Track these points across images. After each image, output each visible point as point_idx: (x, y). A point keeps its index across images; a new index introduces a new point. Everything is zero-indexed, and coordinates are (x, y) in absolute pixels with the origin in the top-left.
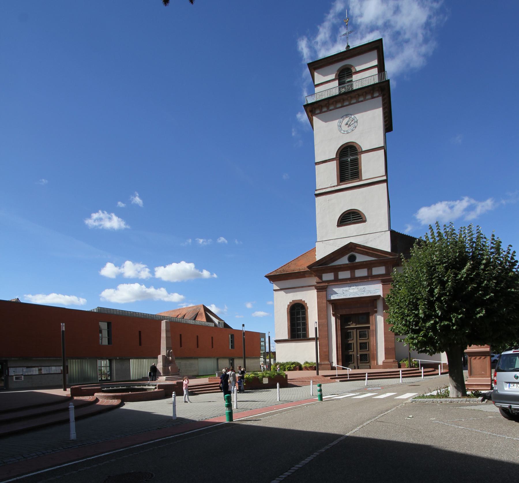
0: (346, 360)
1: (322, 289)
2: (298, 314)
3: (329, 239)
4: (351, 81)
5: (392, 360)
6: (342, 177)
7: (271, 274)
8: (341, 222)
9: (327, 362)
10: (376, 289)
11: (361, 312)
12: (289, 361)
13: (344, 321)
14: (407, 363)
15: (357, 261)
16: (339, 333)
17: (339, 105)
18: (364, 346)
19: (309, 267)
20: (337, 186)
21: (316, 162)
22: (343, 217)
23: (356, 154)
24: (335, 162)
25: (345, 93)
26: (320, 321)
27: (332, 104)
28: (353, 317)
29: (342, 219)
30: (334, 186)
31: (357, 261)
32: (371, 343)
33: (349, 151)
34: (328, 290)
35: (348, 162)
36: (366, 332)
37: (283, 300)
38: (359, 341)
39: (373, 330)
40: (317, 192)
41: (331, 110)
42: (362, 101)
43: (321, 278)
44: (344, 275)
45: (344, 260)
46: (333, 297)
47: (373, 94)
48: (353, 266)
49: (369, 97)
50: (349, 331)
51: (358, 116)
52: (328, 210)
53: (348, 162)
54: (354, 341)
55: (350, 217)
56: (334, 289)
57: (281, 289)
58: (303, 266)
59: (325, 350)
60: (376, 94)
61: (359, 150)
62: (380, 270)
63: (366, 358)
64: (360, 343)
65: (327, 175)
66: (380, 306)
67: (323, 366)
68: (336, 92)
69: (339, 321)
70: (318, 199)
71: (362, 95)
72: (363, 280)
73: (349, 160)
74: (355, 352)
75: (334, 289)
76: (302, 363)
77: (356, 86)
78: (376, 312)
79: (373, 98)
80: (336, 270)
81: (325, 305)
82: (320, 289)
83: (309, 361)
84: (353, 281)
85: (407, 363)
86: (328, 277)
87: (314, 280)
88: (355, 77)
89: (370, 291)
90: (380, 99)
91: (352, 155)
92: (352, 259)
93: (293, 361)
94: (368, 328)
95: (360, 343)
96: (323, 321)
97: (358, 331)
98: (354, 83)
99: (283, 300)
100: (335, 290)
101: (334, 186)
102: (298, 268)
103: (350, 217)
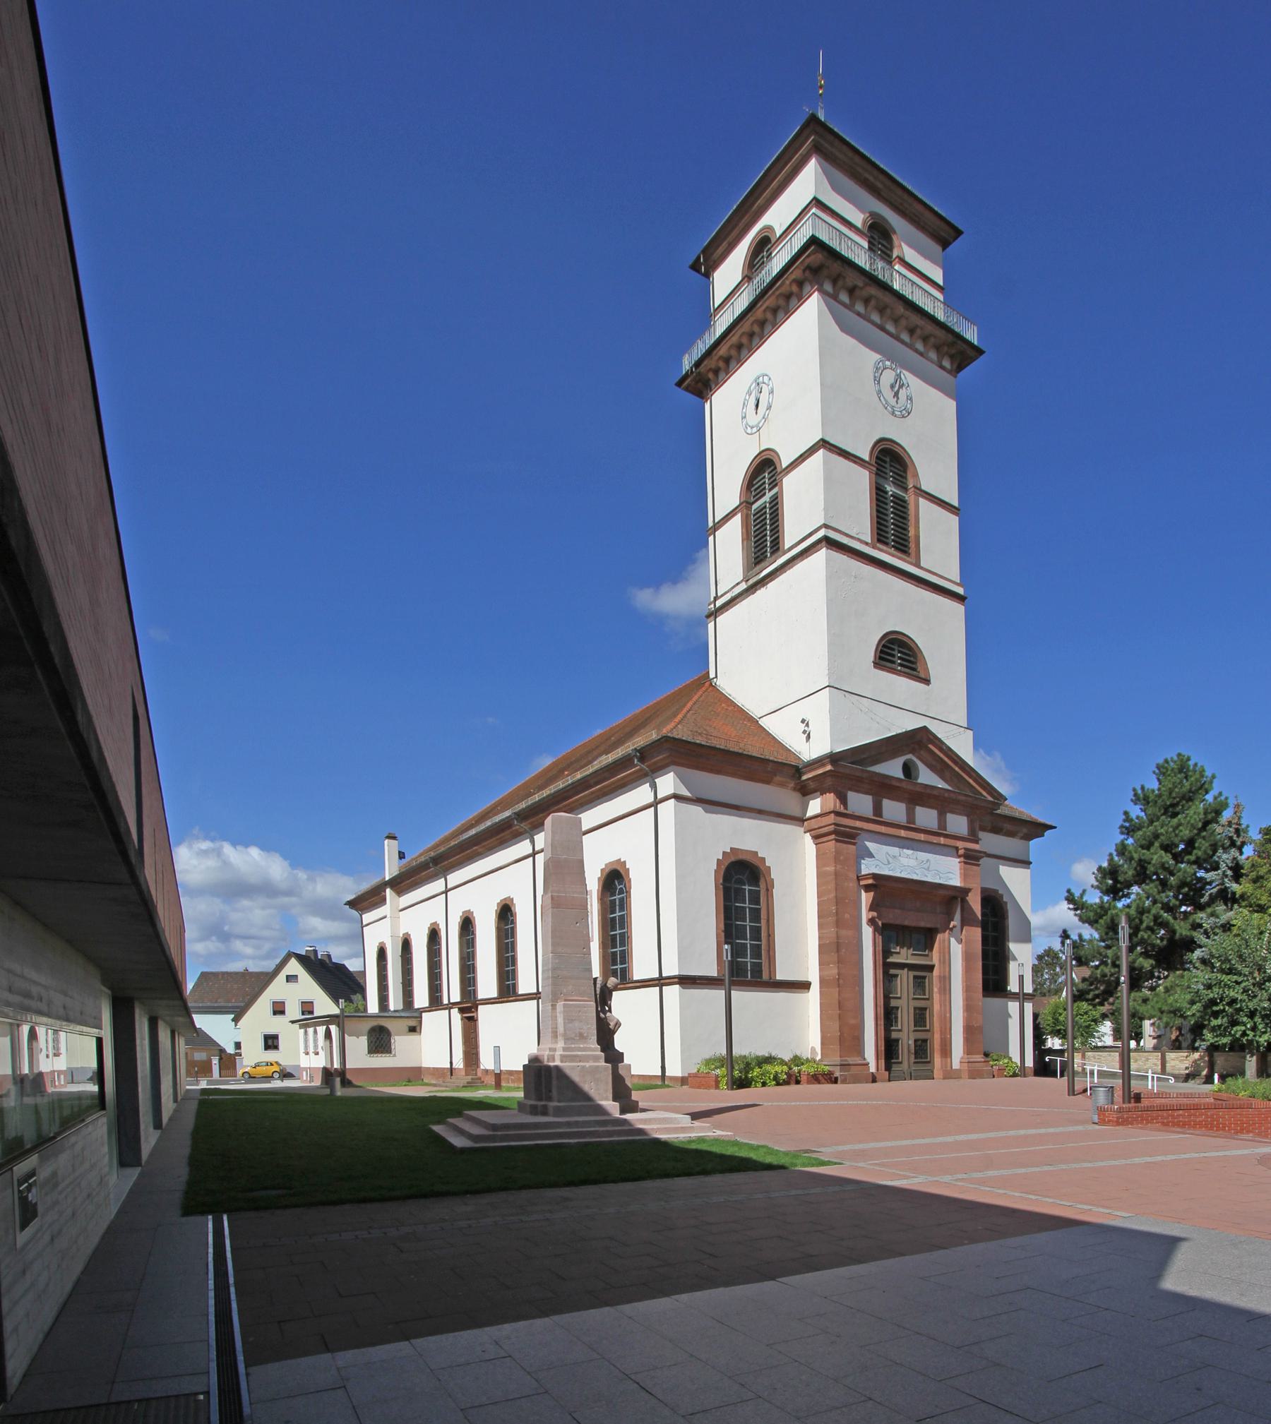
1: (842, 835)
45: (893, 768)
46: (867, 867)
80: (882, 788)
86: (861, 803)
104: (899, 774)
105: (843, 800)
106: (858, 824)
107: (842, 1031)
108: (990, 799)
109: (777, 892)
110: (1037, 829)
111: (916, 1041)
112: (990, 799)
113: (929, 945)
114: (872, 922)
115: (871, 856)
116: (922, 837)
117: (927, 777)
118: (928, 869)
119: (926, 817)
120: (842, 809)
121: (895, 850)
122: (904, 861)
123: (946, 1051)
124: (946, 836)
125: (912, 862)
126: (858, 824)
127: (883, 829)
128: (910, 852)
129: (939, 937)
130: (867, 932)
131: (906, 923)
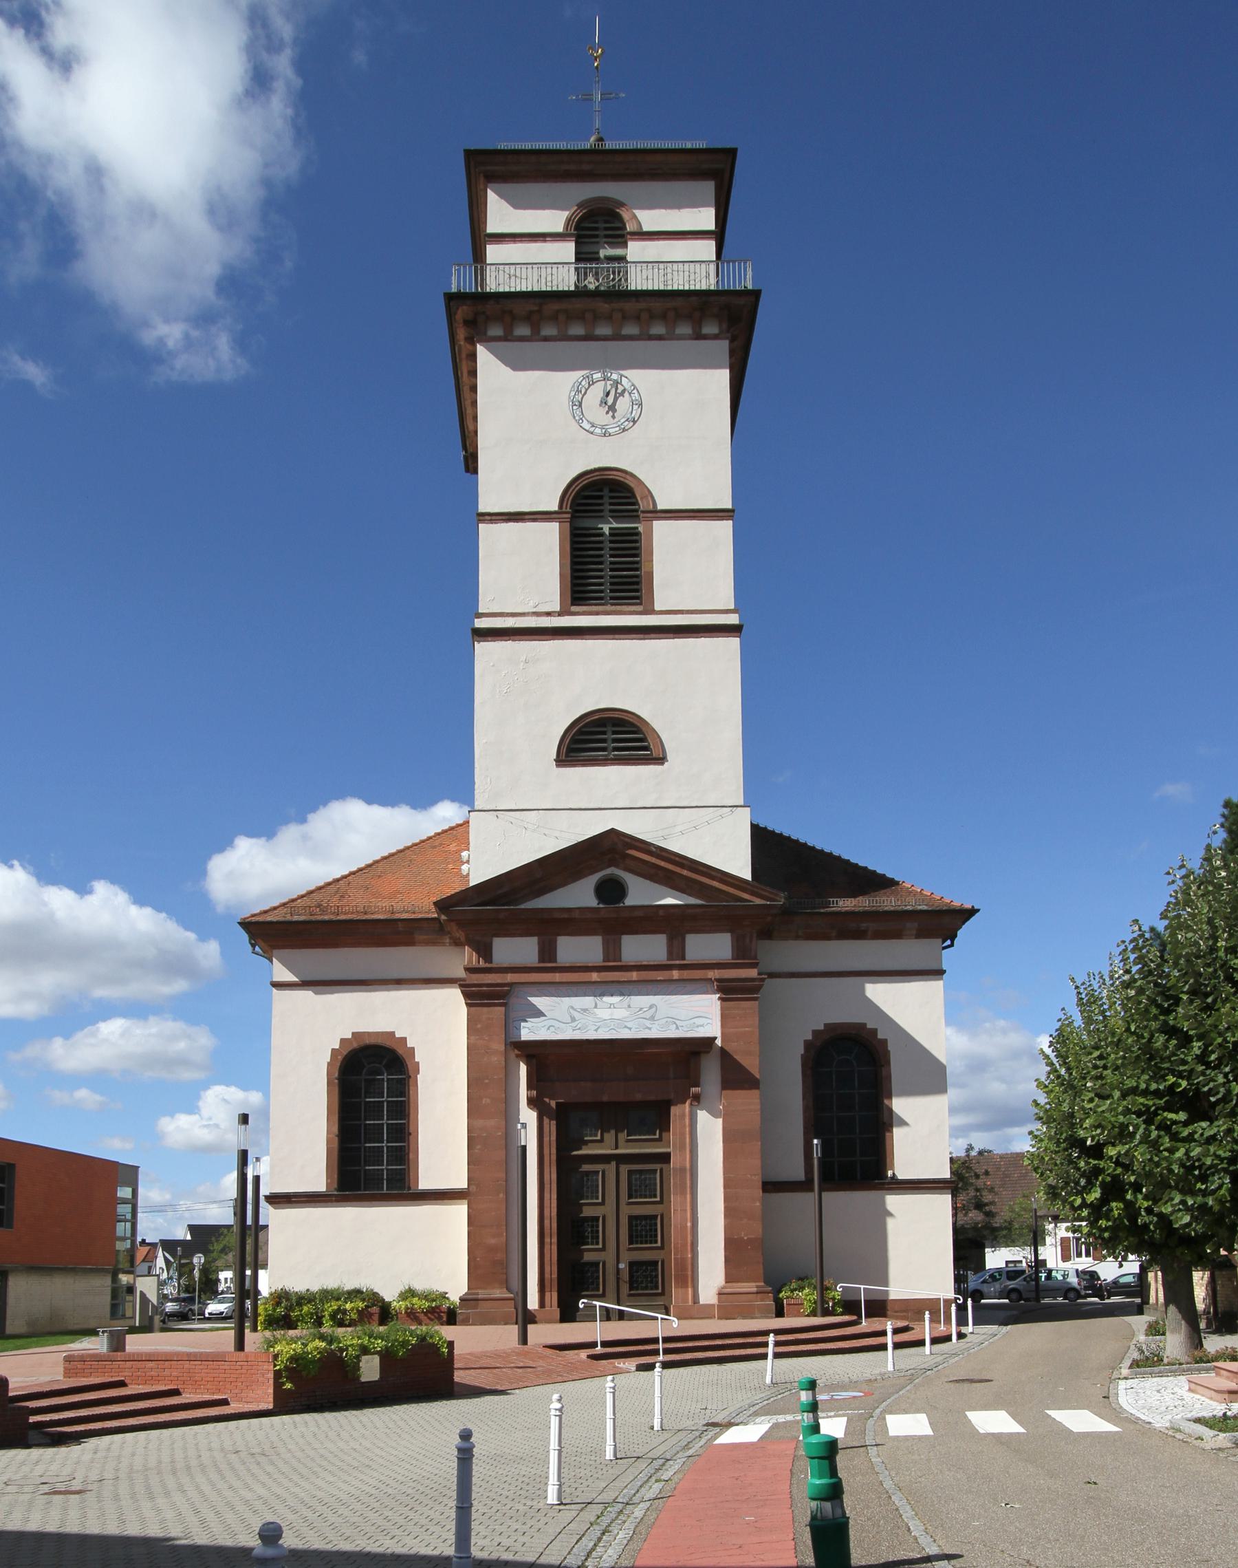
0: (573, 1285)
1: (489, 996)
2: (373, 1087)
3: (523, 810)
4: (622, 259)
5: (751, 1287)
6: (579, 589)
7: (269, 918)
8: (570, 750)
9: (498, 1293)
10: (695, 1015)
11: (639, 1097)
12: (331, 1284)
13: (567, 1123)
14: (807, 1295)
15: (629, 901)
16: (552, 1175)
17: (577, 330)
18: (646, 1229)
19: (443, 905)
20: (560, 614)
21: (481, 509)
22: (580, 732)
23: (634, 515)
24: (553, 529)
25: (596, 294)
26: (479, 1123)
27: (554, 318)
28: (605, 1108)
29: (574, 741)
30: (548, 614)
31: (629, 901)
32: (675, 1219)
33: (606, 500)
34: (513, 1001)
35: (604, 535)
36: (654, 1177)
37: (313, 1027)
38: (626, 1211)
39: (683, 1170)
40: (481, 623)
41: (546, 339)
42: (660, 338)
43: (485, 951)
44: (578, 949)
45: (580, 895)
46: (530, 1031)
47: (697, 325)
48: (614, 919)
49: (684, 329)
50: (586, 1167)
51: (641, 379)
52: (522, 697)
53: (604, 535)
54: (608, 1207)
55: (605, 737)
56: (533, 1000)
57: (305, 984)
58: (419, 901)
59: (493, 1241)
60: (710, 328)
61: (643, 505)
62: (713, 946)
63: (651, 1280)
64: (632, 1218)
65: (520, 569)
66: (711, 1073)
67: (484, 1307)
68: (566, 280)
69: (551, 1126)
70: (485, 651)
71: (663, 317)
72: (650, 978)
73: (606, 529)
74: (611, 1253)
75: (533, 1000)
76: (389, 1294)
77: (638, 280)
78: (697, 1098)
79: (698, 336)
80: (550, 927)
81: (497, 1060)
82: (476, 997)
83: (420, 1286)
84: (613, 976)
85: (807, 1295)
86: (515, 950)
87: (459, 960)
88: (635, 250)
89: (674, 1020)
90: (723, 346)
91: (618, 515)
92: (611, 891)
93: (349, 1286)
94: (665, 1158)
95: (632, 1218)
96: (491, 1123)
97: (624, 1169)
98: (632, 269)
99: (313, 1027)
100: (539, 1002)
101: (548, 614)
102: (385, 904)
103: (605, 737)
104: (591, 901)
105: (485, 951)
106: (510, 978)
107: (491, 1260)
108: (758, 901)
109: (422, 1079)
110: (944, 923)
111: (632, 1265)
112: (758, 901)
113: (663, 1123)
114: (531, 1102)
115: (539, 1014)
116: (634, 975)
117: (642, 893)
118: (652, 1018)
119: (644, 948)
120: (482, 964)
121: (587, 1001)
122: (603, 1013)
123: (689, 1276)
124: (682, 967)
125: (620, 1013)
126: (510, 978)
127: (557, 977)
128: (615, 999)
129: (675, 1110)
130: (528, 1116)
131: (605, 1098)
